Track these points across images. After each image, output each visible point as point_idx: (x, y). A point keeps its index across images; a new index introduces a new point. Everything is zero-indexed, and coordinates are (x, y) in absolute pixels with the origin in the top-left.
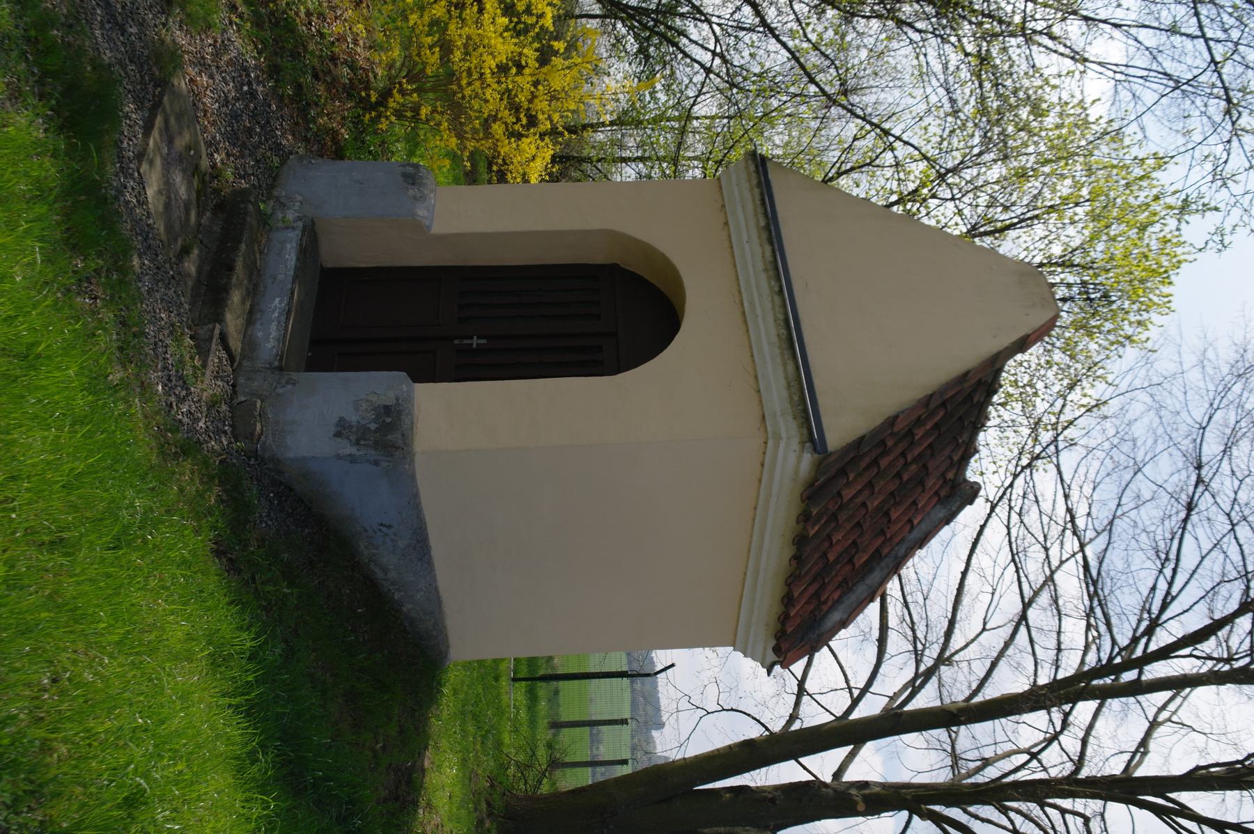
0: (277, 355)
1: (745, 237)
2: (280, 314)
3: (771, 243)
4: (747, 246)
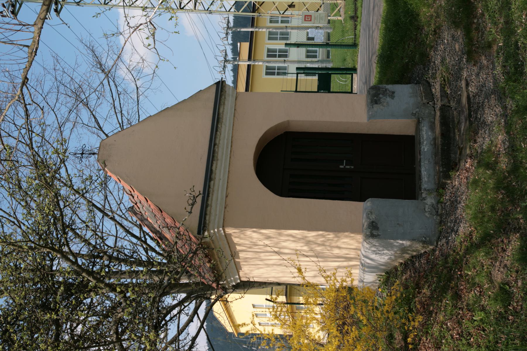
0: (421, 123)
1: (221, 181)
2: (423, 143)
3: (211, 170)
4: (222, 176)
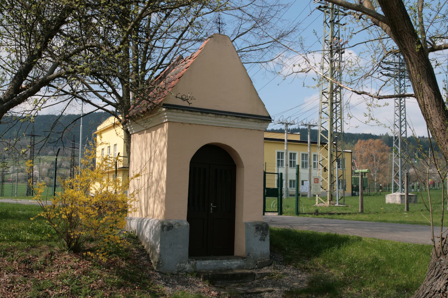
0: (243, 260)
1: (201, 120)
2: (229, 261)
3: (208, 113)
